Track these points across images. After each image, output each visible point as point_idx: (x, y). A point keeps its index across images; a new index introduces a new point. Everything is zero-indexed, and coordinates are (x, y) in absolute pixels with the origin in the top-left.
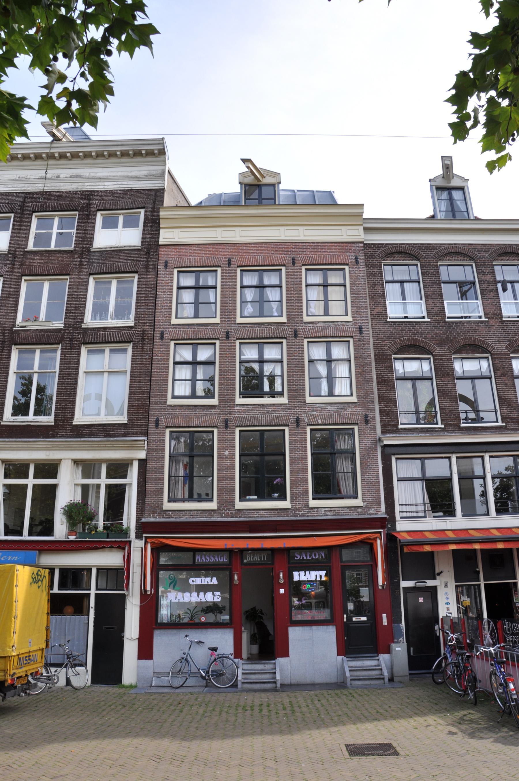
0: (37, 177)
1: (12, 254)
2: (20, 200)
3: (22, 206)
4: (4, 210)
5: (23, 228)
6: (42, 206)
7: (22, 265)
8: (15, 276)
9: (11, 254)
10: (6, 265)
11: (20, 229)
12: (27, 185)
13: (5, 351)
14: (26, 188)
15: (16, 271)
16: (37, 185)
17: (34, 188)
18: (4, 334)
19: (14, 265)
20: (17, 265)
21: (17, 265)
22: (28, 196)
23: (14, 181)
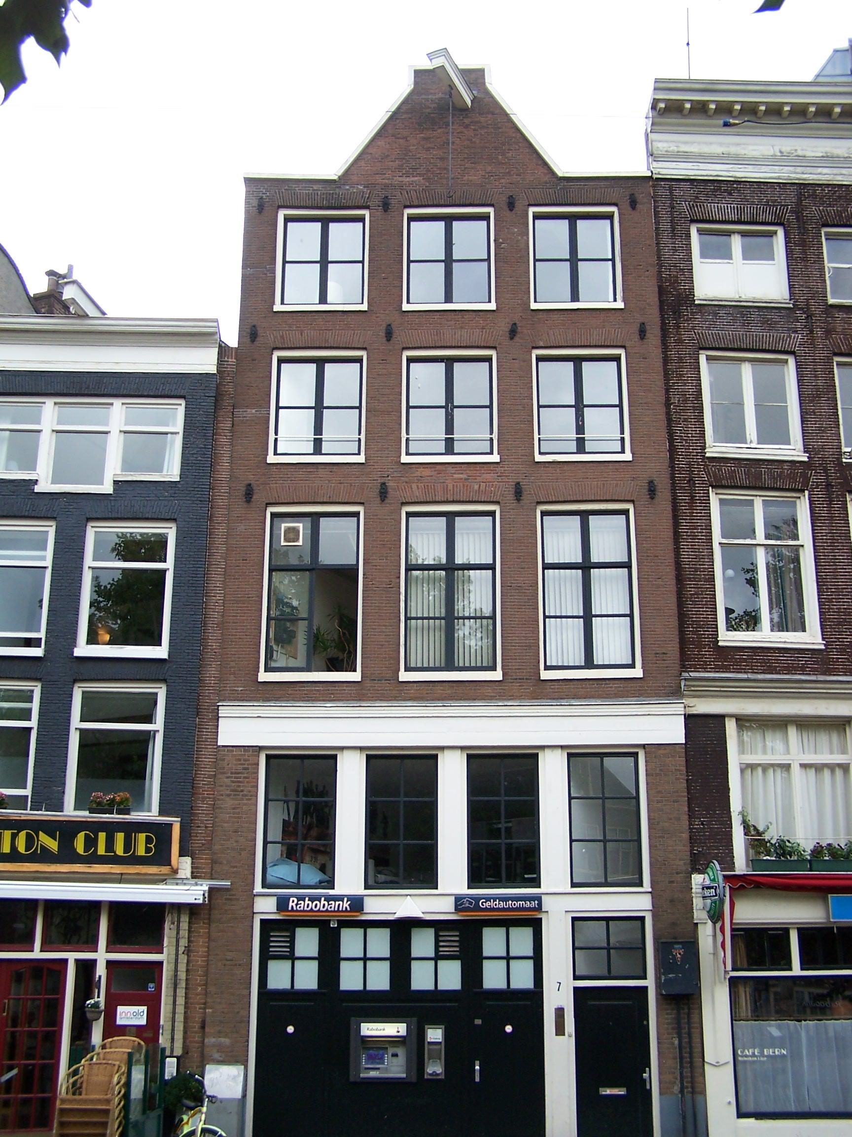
0: (821, 155)
1: (802, 309)
2: (790, 199)
3: (798, 212)
4: (761, 218)
5: (812, 258)
6: (839, 214)
7: (828, 332)
8: (821, 354)
9: (799, 309)
10: (796, 332)
11: (804, 259)
12: (799, 169)
13: (836, 506)
14: (798, 176)
15: (819, 343)
16: (820, 170)
17: (815, 177)
18: (826, 470)
19: (812, 332)
20: (819, 332)
21: (819, 332)
22: (804, 190)
23: (782, 159)
